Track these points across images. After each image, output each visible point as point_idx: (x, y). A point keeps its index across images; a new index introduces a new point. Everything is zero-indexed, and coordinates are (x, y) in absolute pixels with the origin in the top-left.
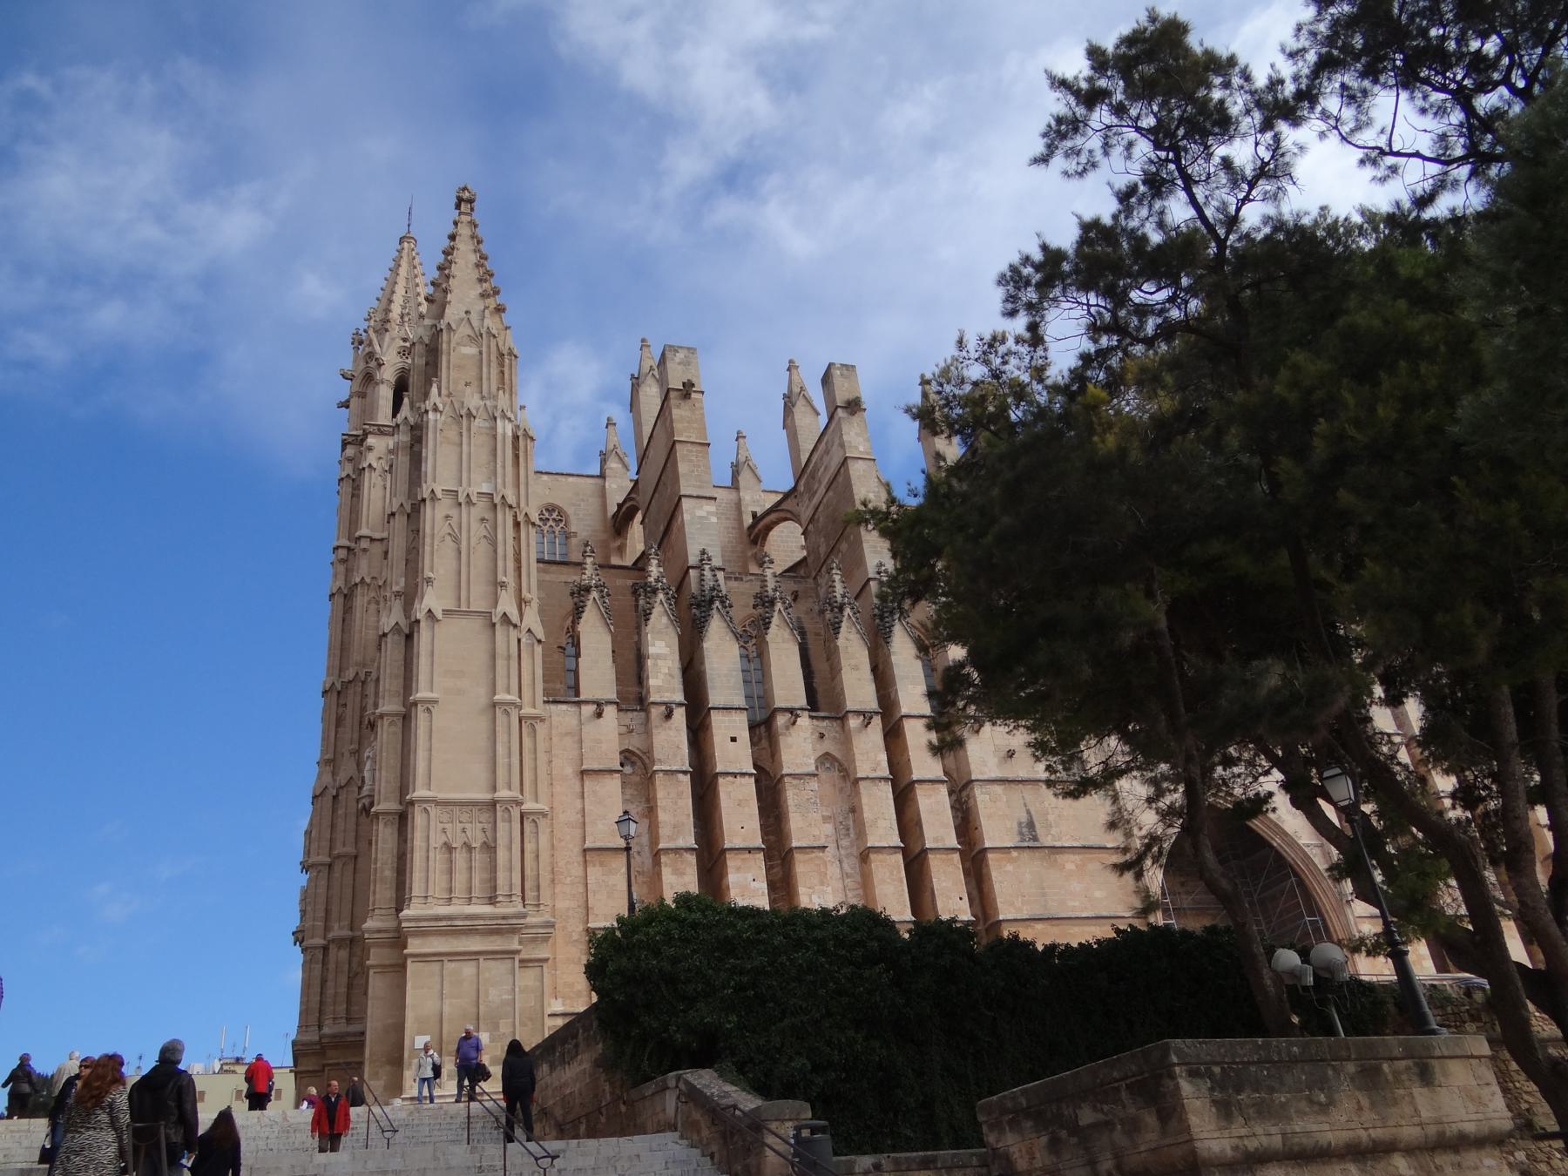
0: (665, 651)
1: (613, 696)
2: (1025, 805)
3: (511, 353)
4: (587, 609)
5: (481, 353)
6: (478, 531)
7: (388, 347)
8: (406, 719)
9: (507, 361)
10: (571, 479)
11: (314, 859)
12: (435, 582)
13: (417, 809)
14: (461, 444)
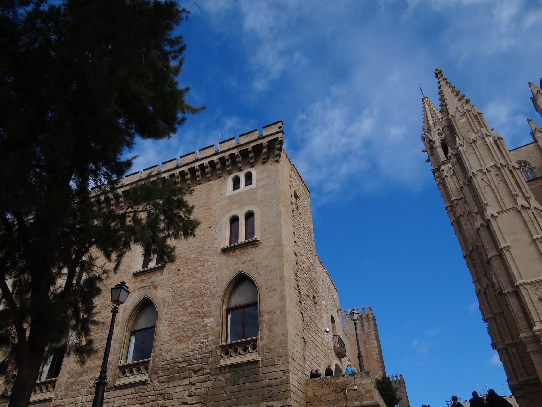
3: (479, 113)
5: (468, 119)
6: (496, 180)
7: (434, 135)
8: (501, 256)
9: (479, 117)
10: (523, 148)
11: (487, 317)
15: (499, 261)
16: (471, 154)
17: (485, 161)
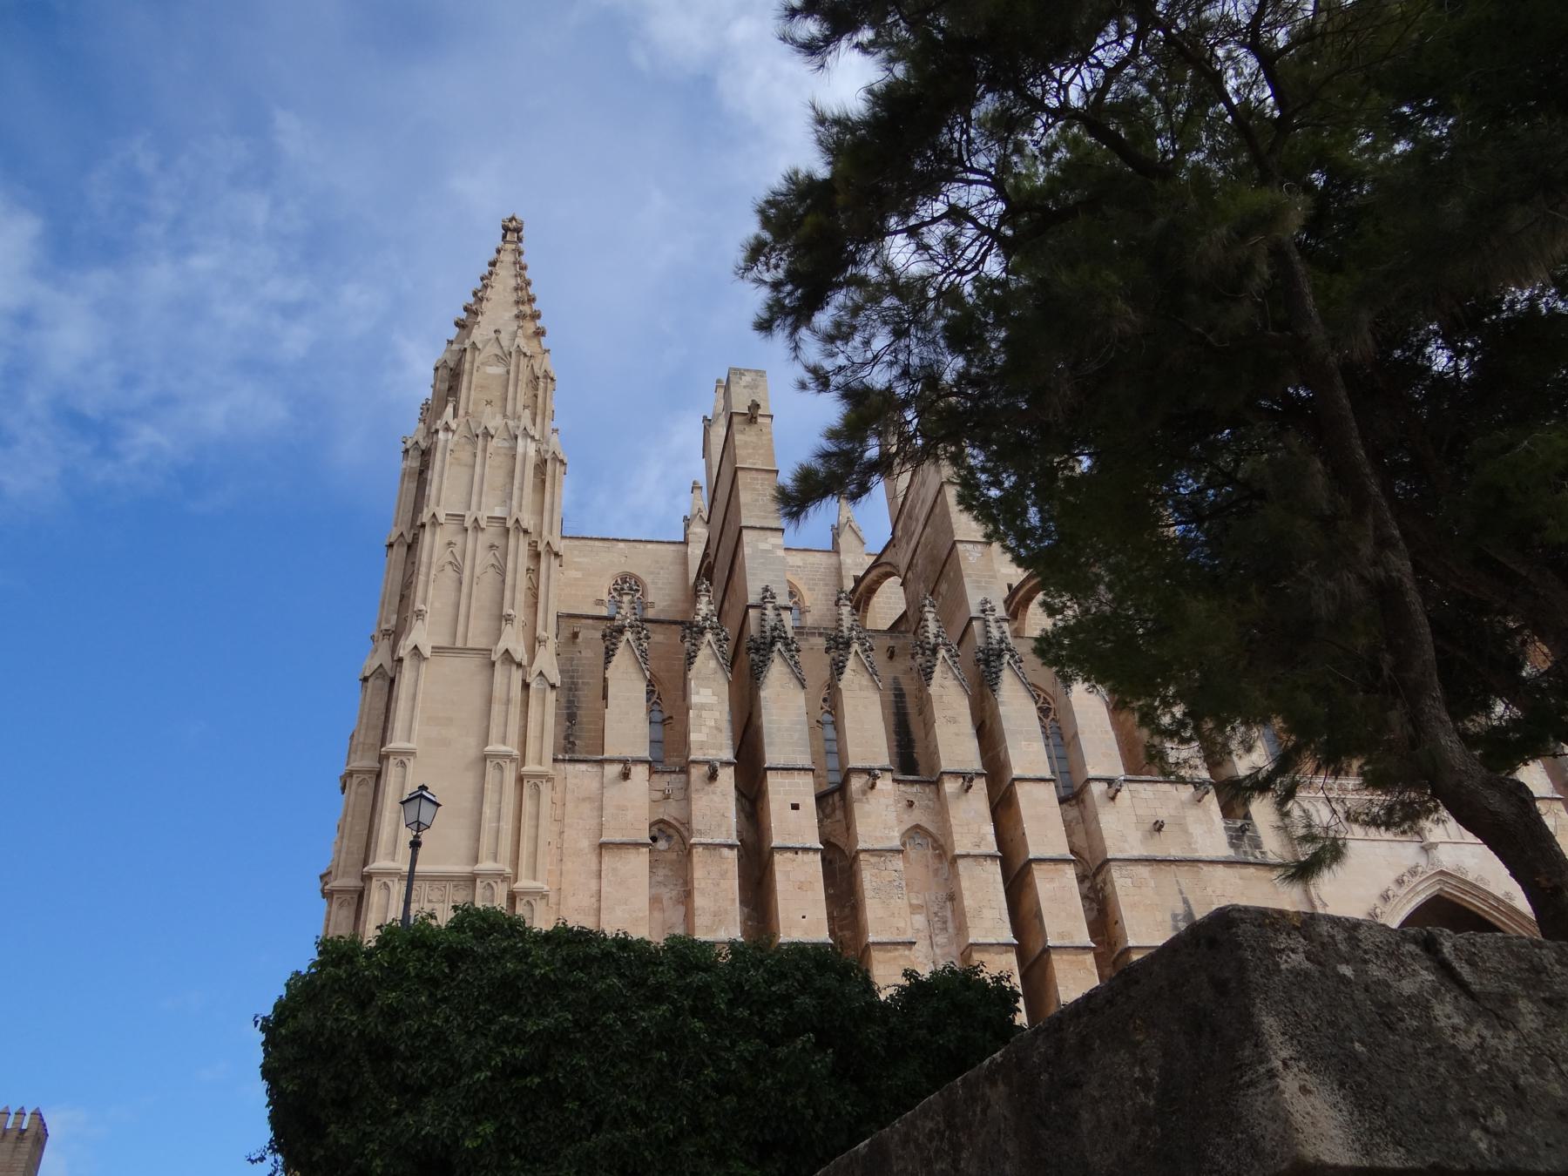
0: (713, 700)
1: (645, 753)
2: (1181, 892)
3: (547, 375)
4: (618, 652)
5: (508, 372)
6: (484, 558)
9: (542, 384)
10: (650, 546)
12: (427, 617)
13: (375, 883)
14: (474, 466)
15: (368, 789)
16: (459, 464)
17: (484, 499)
